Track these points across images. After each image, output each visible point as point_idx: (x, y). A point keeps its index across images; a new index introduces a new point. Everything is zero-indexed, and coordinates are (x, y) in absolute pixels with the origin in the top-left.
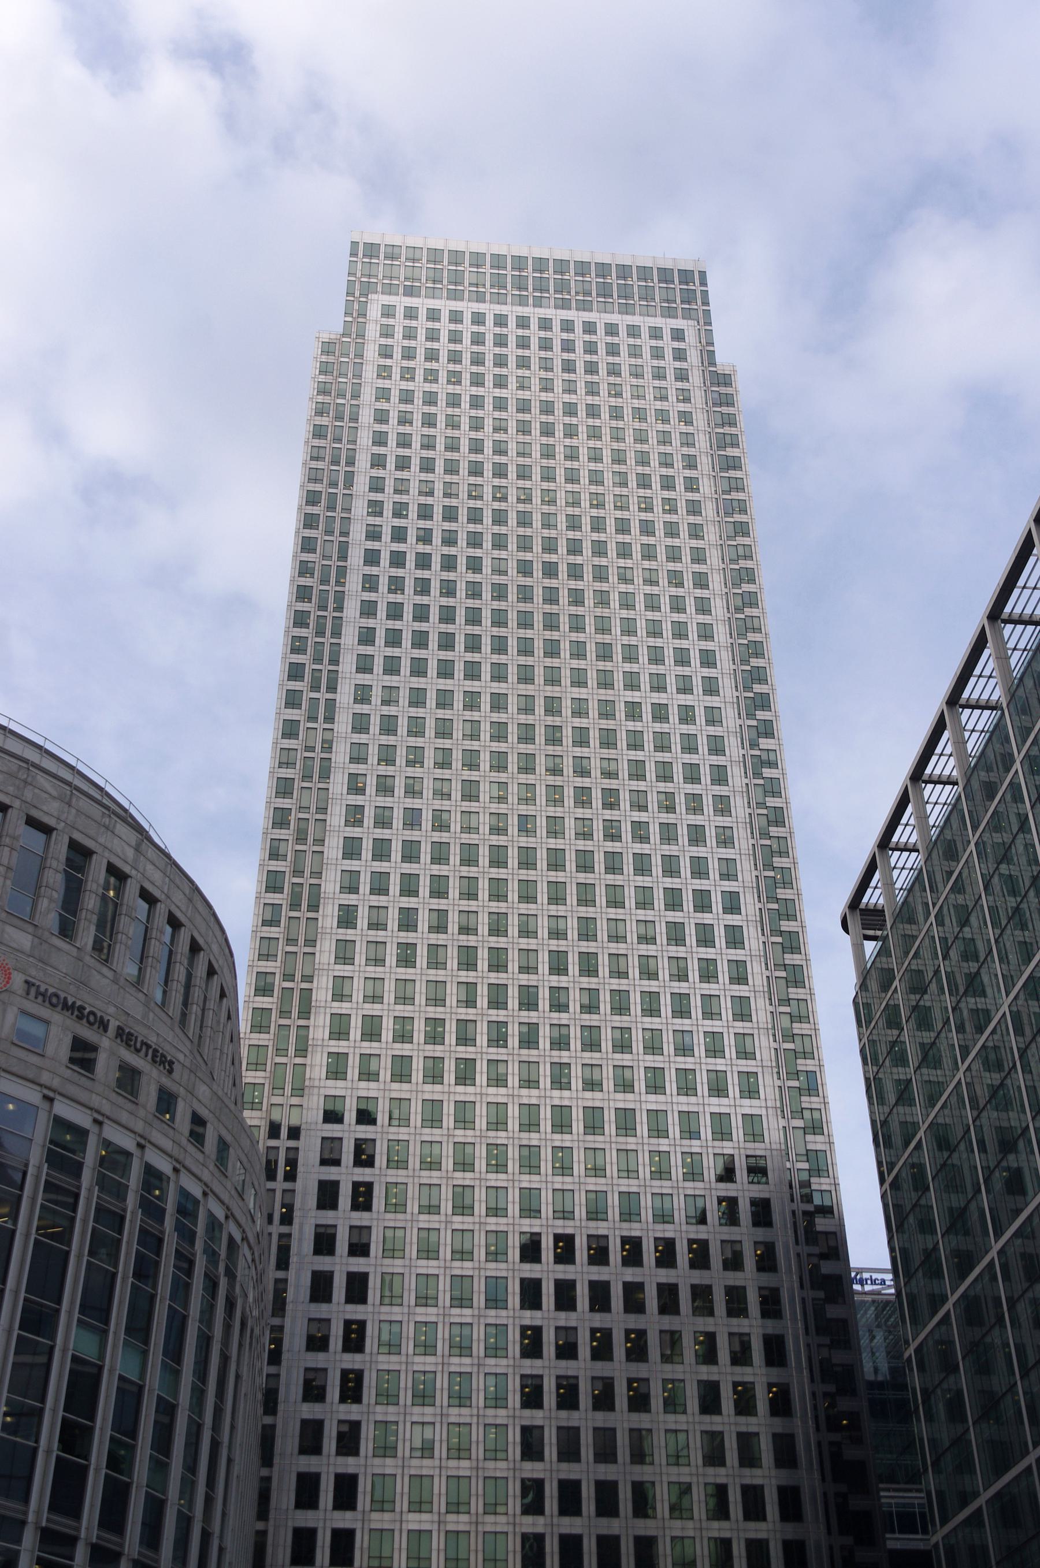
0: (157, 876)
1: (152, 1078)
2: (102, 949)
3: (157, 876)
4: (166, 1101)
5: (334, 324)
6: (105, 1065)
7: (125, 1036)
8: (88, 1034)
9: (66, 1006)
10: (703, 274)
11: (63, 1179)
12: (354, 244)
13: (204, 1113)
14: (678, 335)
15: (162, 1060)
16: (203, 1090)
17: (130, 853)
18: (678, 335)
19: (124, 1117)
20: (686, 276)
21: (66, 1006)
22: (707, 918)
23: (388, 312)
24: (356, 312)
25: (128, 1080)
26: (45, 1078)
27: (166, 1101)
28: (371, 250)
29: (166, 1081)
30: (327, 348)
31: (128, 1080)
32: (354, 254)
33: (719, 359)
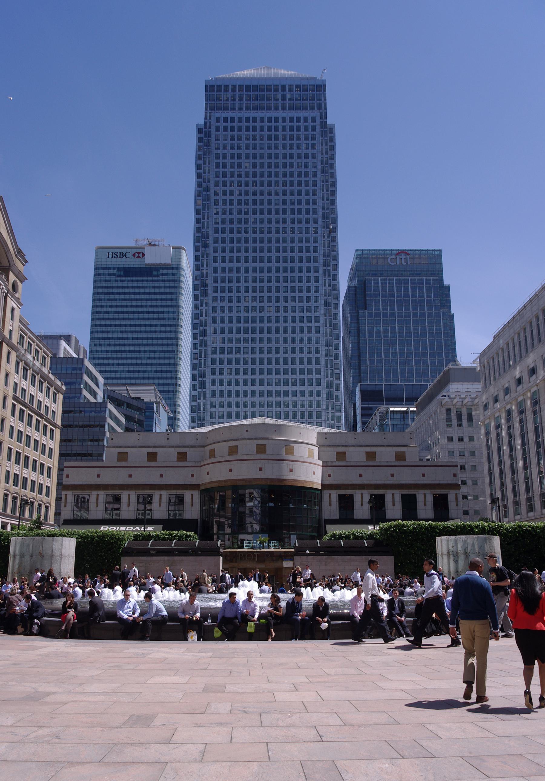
5: (202, 121)
12: (206, 86)
14: (313, 119)
18: (313, 119)
20: (319, 86)
23: (218, 120)
24: (207, 117)
28: (212, 87)
30: (200, 131)
32: (206, 91)
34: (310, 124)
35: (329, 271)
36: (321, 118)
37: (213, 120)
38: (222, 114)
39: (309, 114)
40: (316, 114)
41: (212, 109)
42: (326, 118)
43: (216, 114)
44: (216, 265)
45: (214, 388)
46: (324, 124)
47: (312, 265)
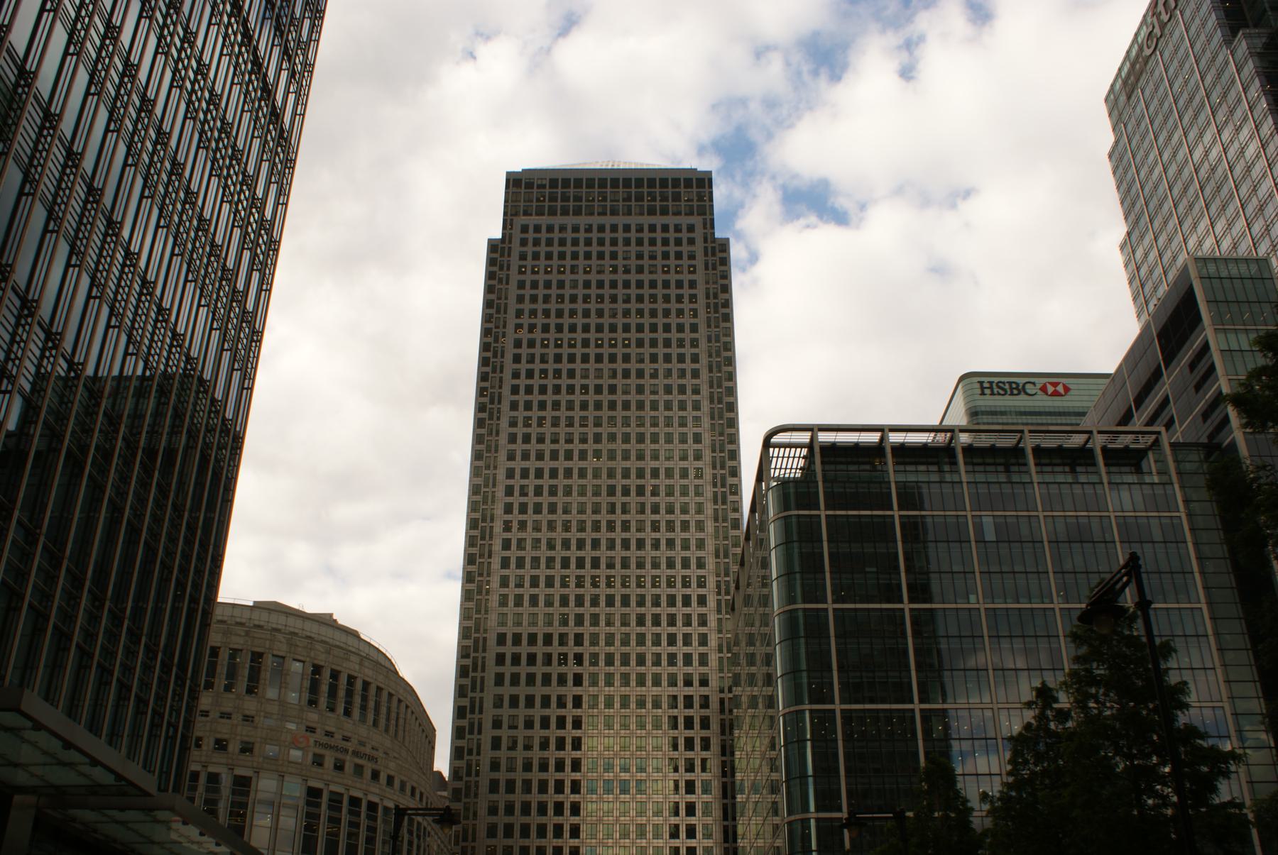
0: (370, 673)
1: (369, 767)
2: (347, 713)
3: (370, 673)
4: (375, 775)
6: (349, 767)
7: (356, 754)
8: (340, 756)
9: (331, 747)
10: (710, 180)
11: (335, 814)
12: (508, 181)
13: (392, 773)
14: (691, 228)
15: (372, 759)
16: (392, 765)
17: (357, 667)
18: (691, 228)
19: (358, 785)
21: (331, 747)
22: (688, 591)
23: (525, 229)
25: (359, 769)
26: (325, 777)
27: (375, 775)
29: (374, 766)
31: (359, 769)
33: (717, 235)
34: (684, 235)
35: (723, 478)
36: (705, 228)
37: (517, 229)
38: (533, 220)
39: (684, 221)
40: (696, 220)
41: (516, 214)
42: (713, 227)
43: (522, 220)
44: (511, 464)
45: (499, 690)
46: (709, 237)
47: (691, 464)
